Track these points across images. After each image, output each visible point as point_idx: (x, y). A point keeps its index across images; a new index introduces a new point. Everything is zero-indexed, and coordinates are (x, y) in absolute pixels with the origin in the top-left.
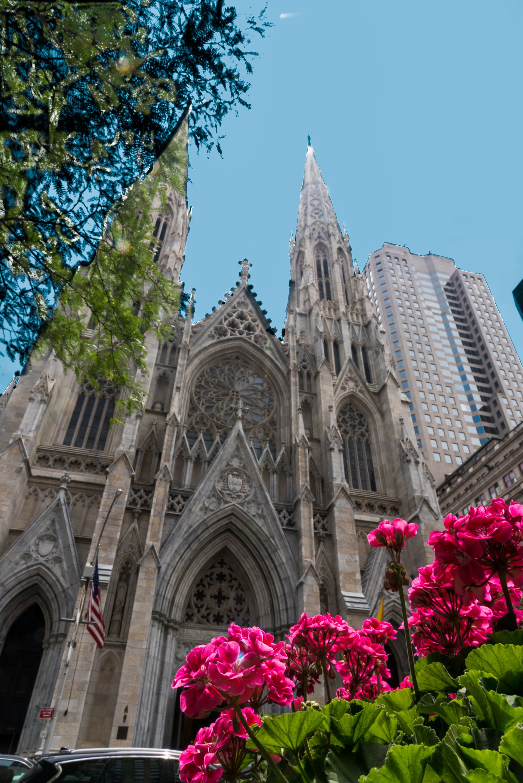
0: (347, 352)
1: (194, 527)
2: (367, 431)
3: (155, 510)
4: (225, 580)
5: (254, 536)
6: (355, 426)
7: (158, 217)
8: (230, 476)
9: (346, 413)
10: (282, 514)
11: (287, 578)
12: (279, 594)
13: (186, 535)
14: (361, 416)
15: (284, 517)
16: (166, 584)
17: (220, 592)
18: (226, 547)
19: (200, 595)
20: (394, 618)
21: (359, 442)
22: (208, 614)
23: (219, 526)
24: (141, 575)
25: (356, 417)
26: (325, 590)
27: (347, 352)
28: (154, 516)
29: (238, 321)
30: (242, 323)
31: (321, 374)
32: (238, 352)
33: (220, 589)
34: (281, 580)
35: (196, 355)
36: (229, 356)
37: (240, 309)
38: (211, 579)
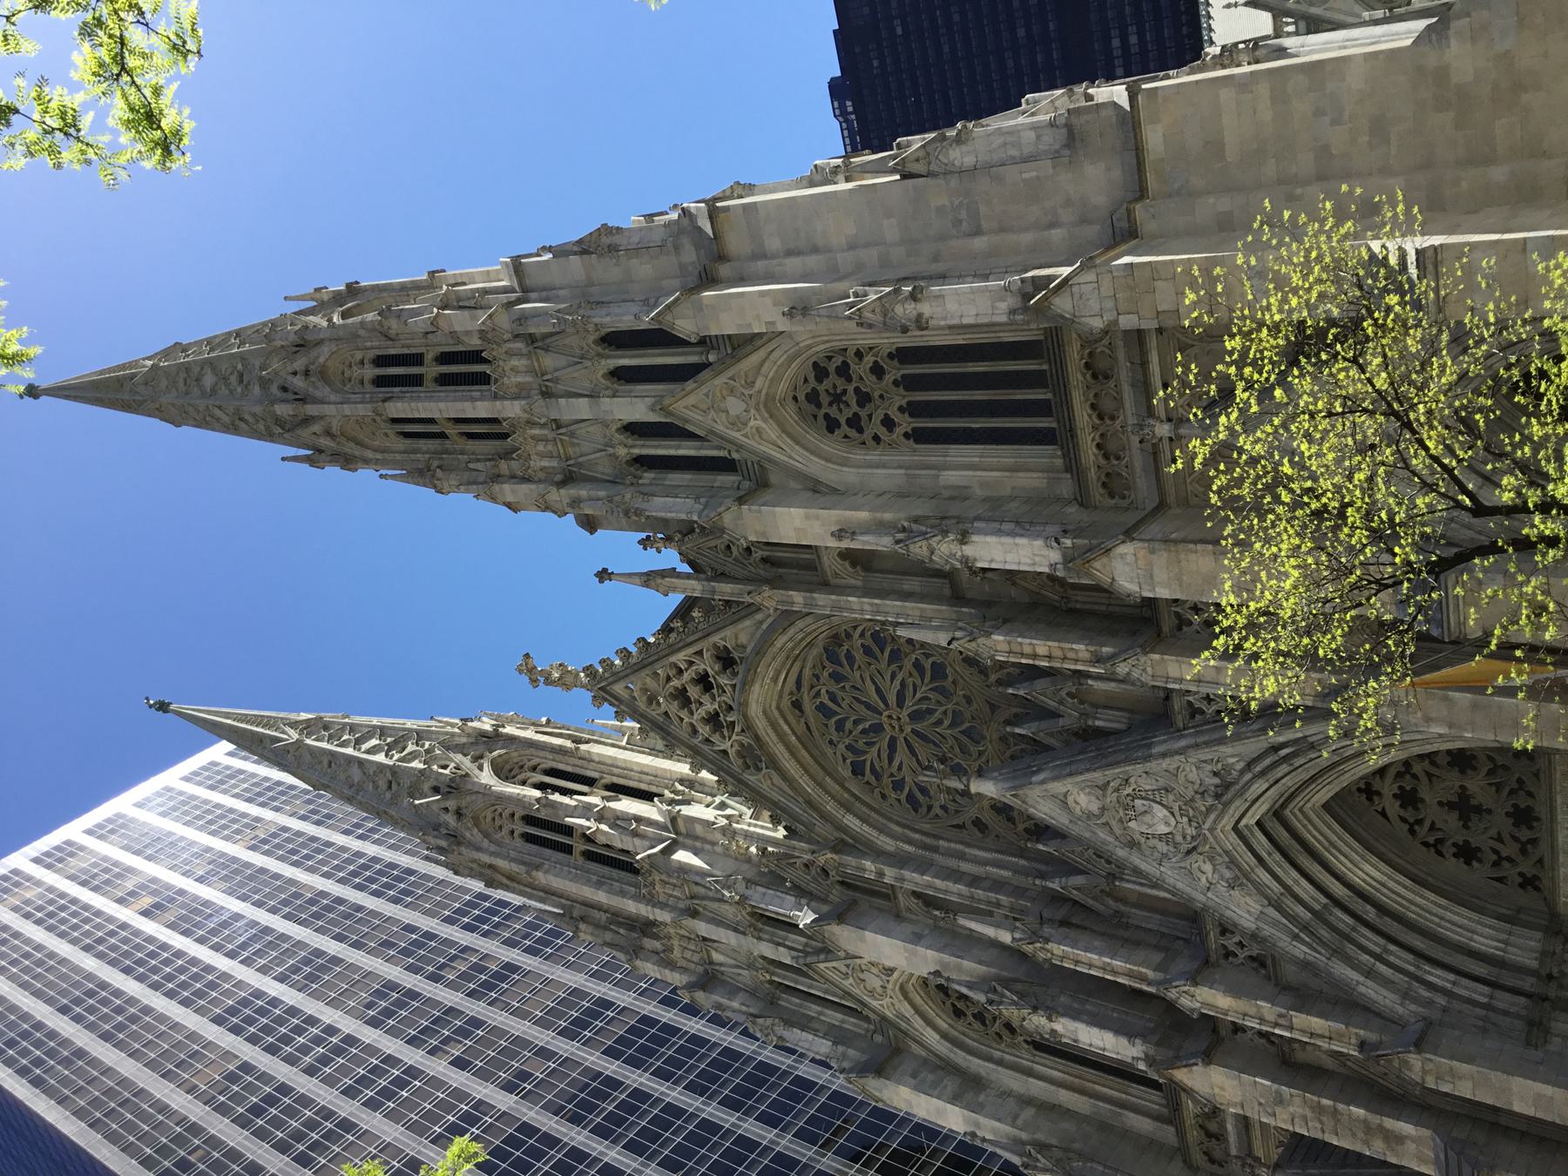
0: (636, 406)
1: (1297, 931)
2: (859, 355)
3: (1276, 1025)
4: (1414, 790)
7: (519, 842)
9: (827, 416)
10: (1198, 705)
13: (1319, 948)
14: (820, 372)
16: (1456, 1005)
17: (1451, 806)
18: (1324, 806)
19: (1467, 853)
21: (909, 383)
22: (1516, 839)
23: (1278, 856)
24: (1446, 1088)
25: (827, 384)
28: (1291, 1028)
31: (753, 538)
32: (778, 708)
33: (1440, 804)
36: (801, 728)
38: (1420, 822)
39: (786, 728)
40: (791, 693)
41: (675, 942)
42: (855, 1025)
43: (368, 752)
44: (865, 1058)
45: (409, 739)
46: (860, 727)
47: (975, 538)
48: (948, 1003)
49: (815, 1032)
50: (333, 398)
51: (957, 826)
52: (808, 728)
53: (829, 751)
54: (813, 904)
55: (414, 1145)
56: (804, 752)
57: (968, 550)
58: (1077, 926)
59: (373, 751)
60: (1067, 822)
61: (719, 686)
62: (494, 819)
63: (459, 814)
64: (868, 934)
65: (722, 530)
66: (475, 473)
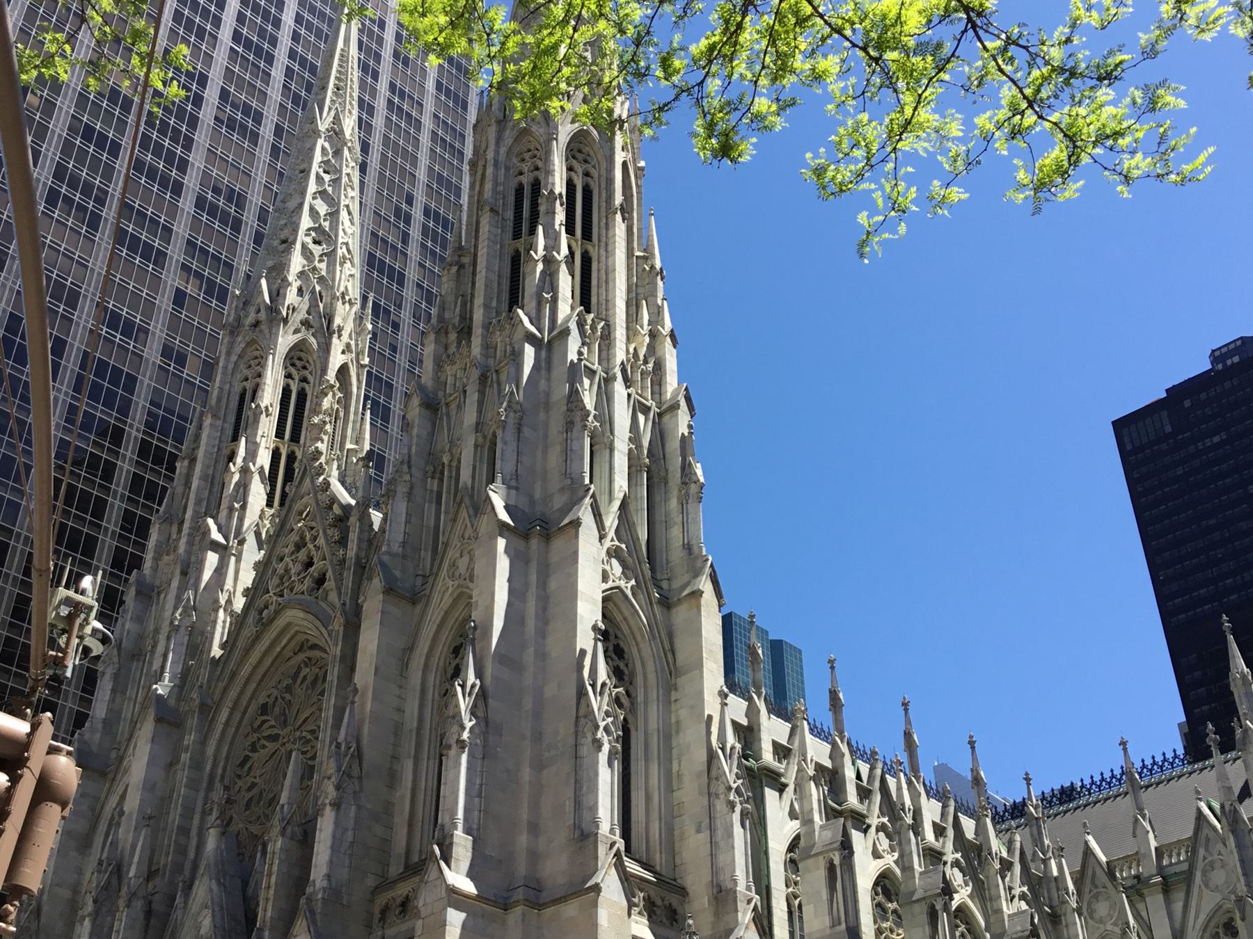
7: (237, 389)
32: (297, 632)
39: (284, 642)
40: (308, 640)
41: (171, 557)
42: (123, 732)
43: (312, 208)
44: (95, 749)
45: (329, 244)
47: (333, 813)
49: (112, 700)
50: (503, 150)
53: (273, 683)
54: (176, 690)
55: (91, 290)
56: (270, 660)
57: (328, 808)
58: (147, 925)
59: (314, 213)
60: (193, 911)
61: (305, 577)
62: (256, 358)
63: (256, 324)
64: (149, 746)
65: (370, 579)
66: (453, 307)
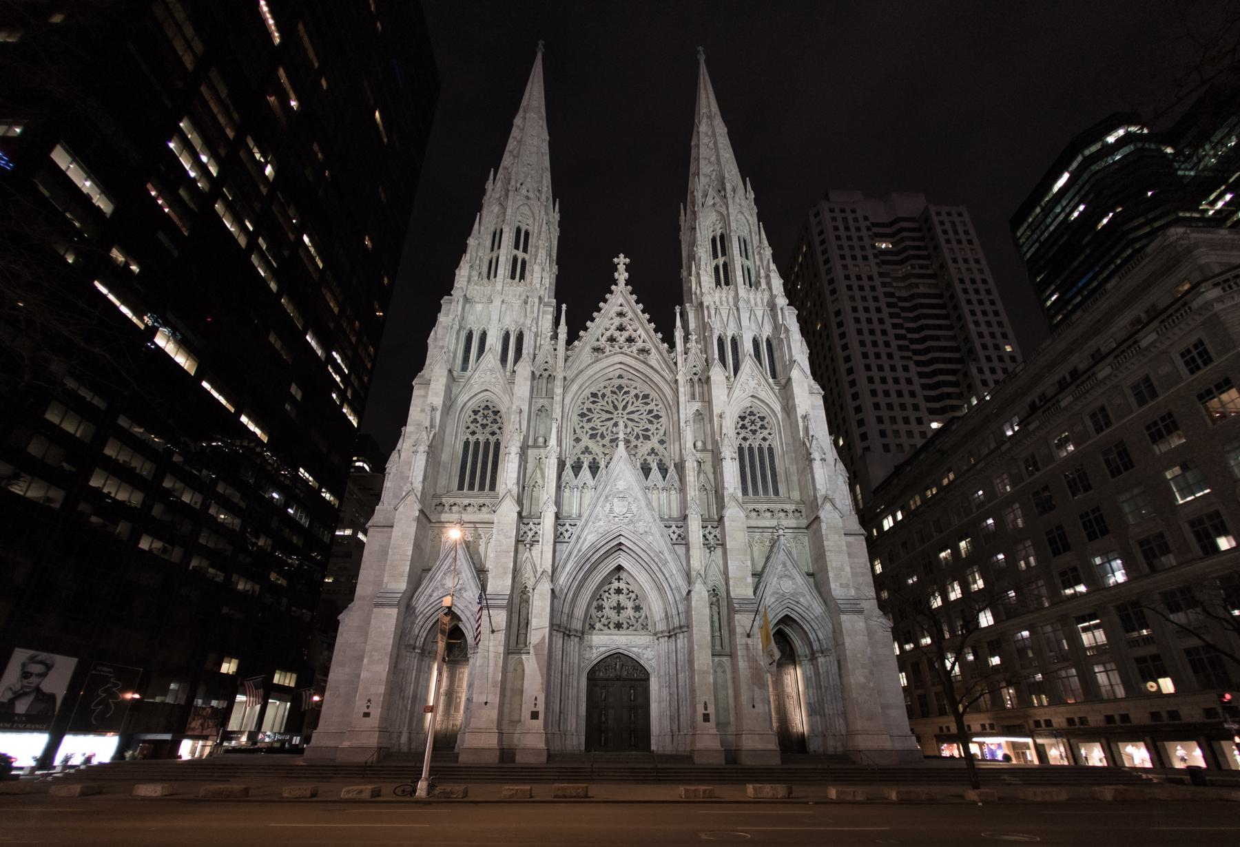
0: (747, 346)
5: (644, 553)
6: (756, 431)
8: (616, 500)
11: (678, 589)
12: (671, 602)
15: (674, 533)
20: (789, 614)
21: (760, 449)
25: (758, 420)
26: (717, 595)
27: (747, 346)
29: (617, 334)
30: (621, 336)
34: (672, 590)
35: (573, 381)
36: (610, 375)
37: (617, 321)
46: (630, 403)
48: (480, 409)
51: (575, 431)
52: (610, 379)
53: (602, 386)
